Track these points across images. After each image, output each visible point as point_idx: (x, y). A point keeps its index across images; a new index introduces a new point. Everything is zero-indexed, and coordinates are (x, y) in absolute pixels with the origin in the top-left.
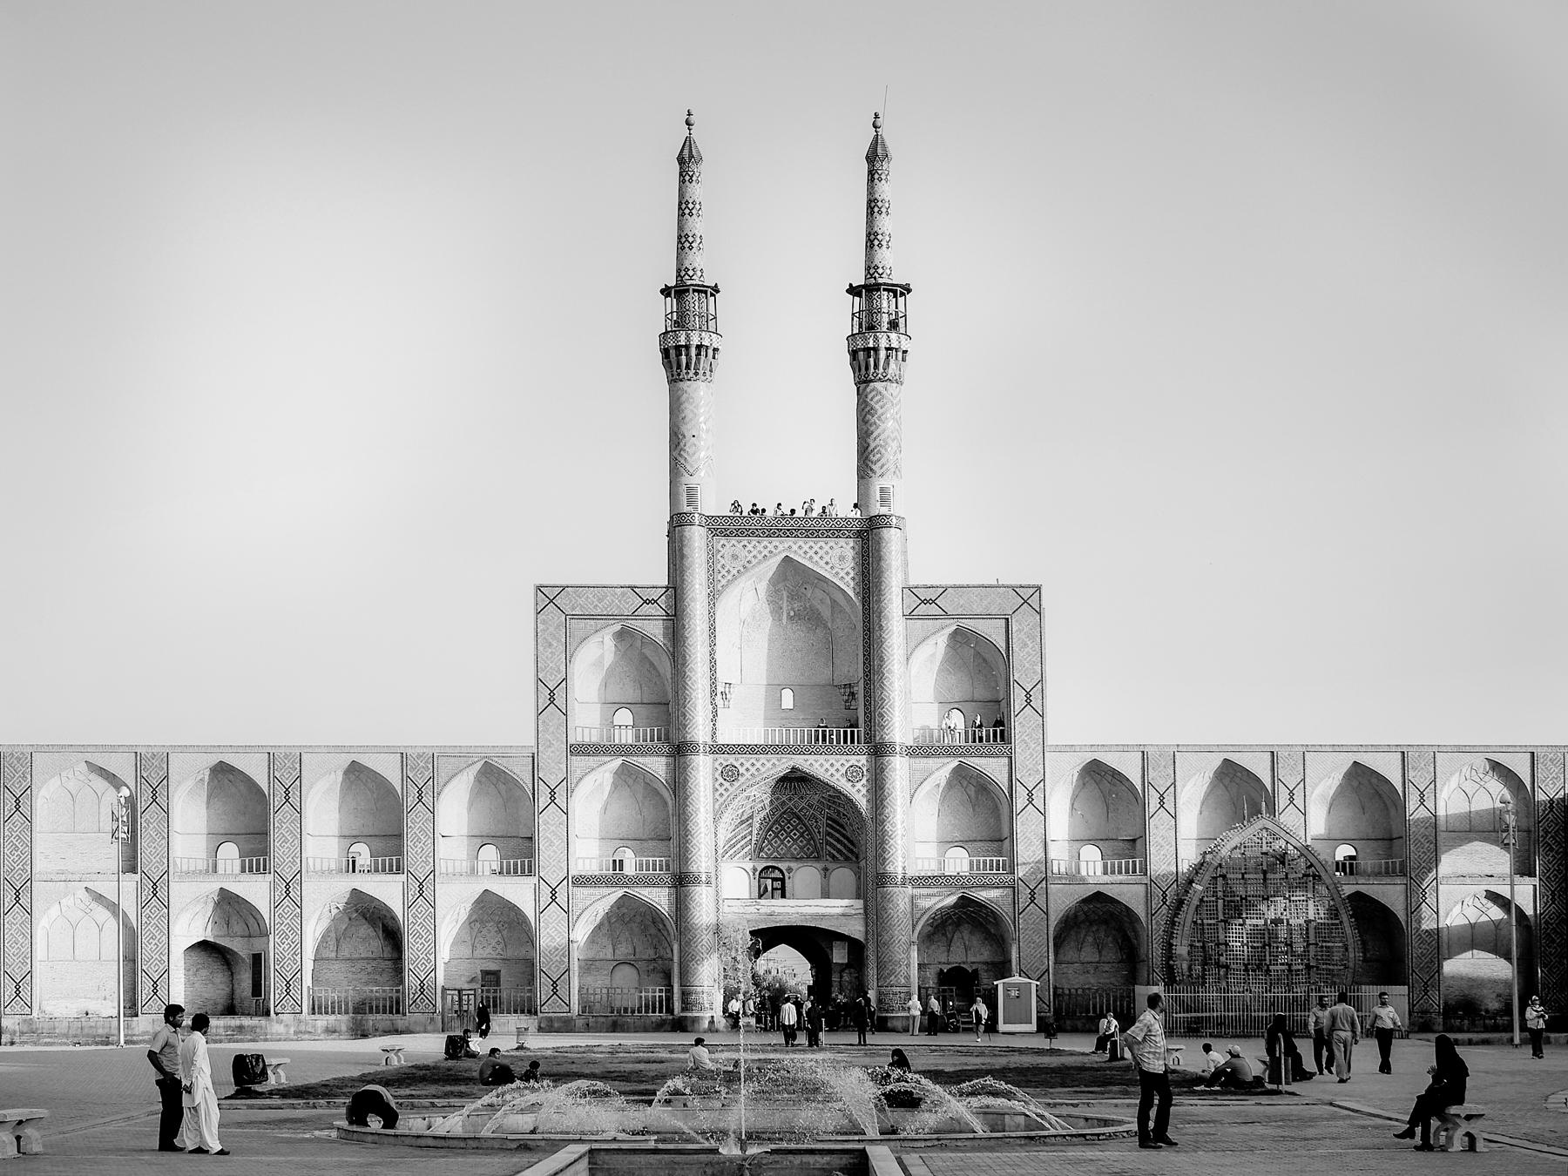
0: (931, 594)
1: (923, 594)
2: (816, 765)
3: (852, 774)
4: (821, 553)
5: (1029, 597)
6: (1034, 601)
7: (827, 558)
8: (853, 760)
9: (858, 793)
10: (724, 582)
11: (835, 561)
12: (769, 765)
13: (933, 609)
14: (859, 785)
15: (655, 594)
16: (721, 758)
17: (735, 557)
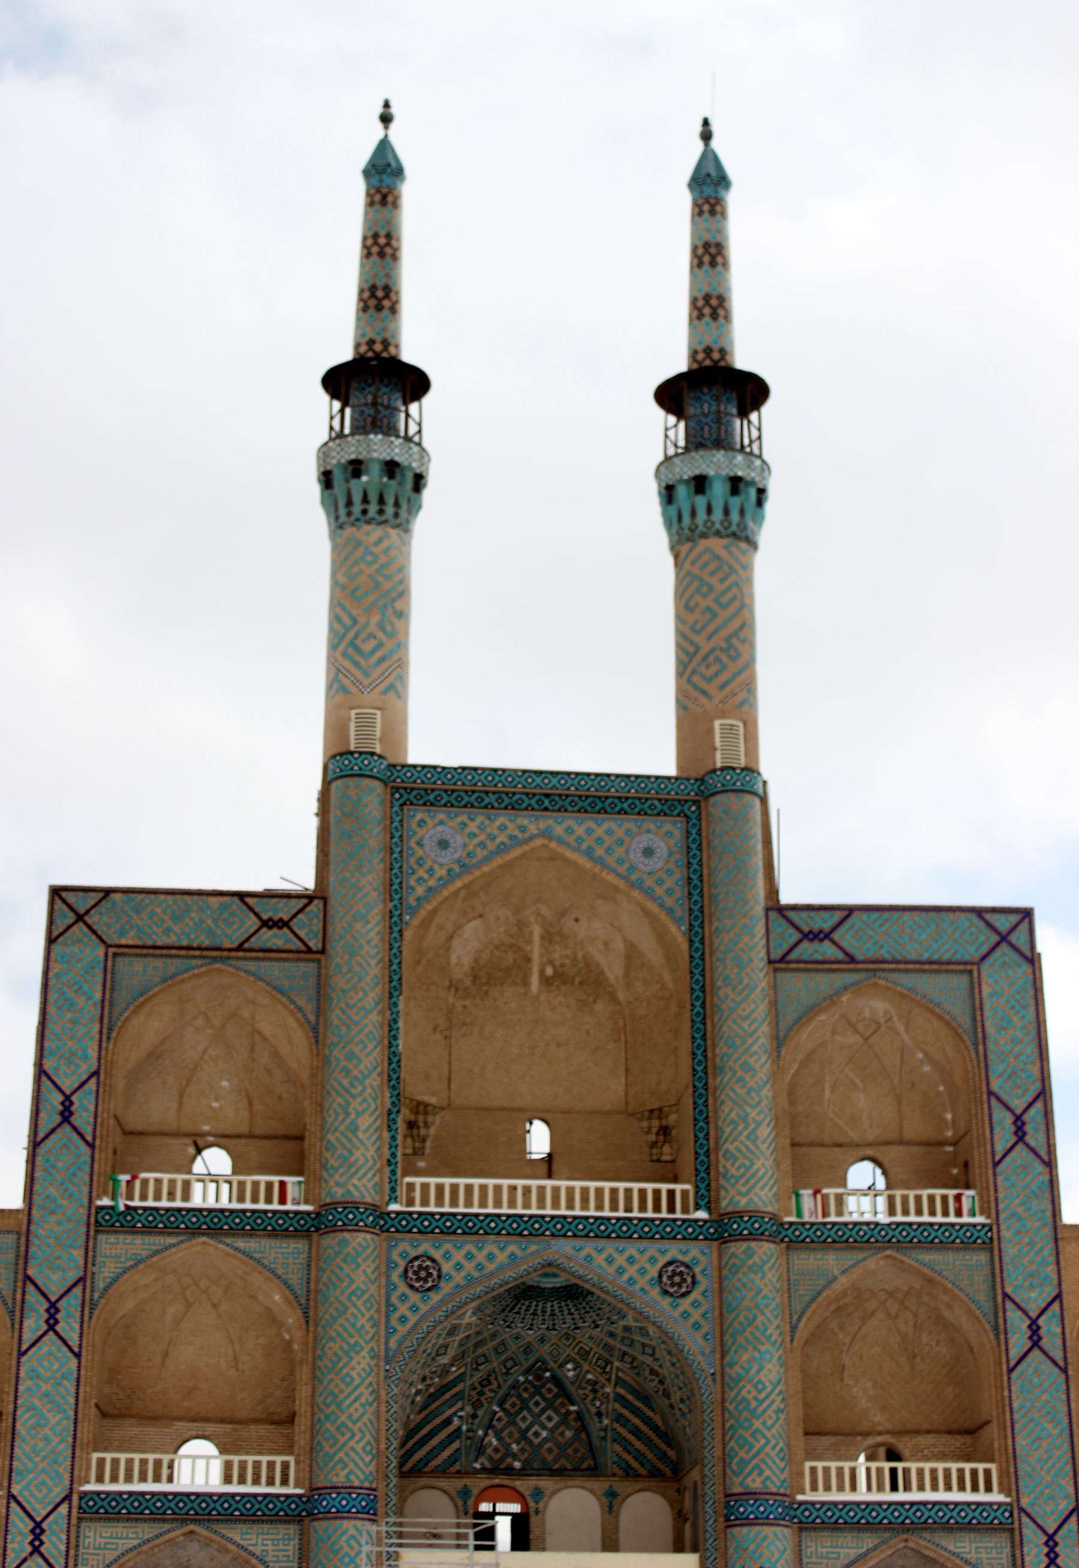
0: (825, 922)
1: (806, 922)
2: (600, 1259)
3: (676, 1280)
4: (609, 840)
5: (1008, 932)
6: (1019, 938)
7: (619, 852)
8: (673, 1250)
9: (684, 1323)
10: (420, 891)
11: (636, 857)
12: (502, 1257)
13: (827, 950)
14: (685, 1303)
15: (284, 910)
16: (406, 1247)
17: (443, 844)
